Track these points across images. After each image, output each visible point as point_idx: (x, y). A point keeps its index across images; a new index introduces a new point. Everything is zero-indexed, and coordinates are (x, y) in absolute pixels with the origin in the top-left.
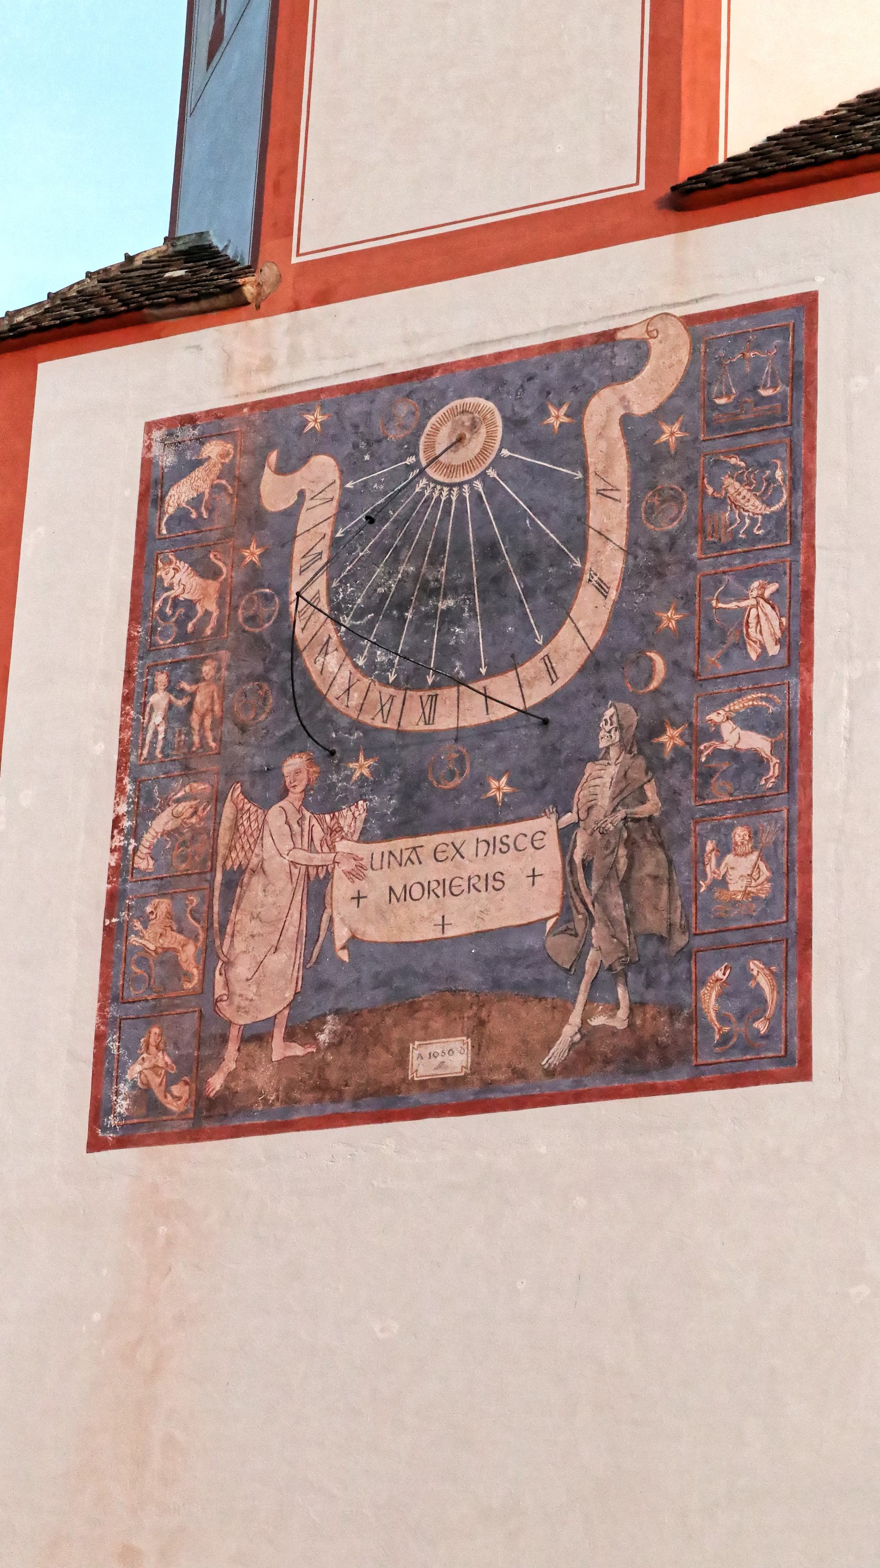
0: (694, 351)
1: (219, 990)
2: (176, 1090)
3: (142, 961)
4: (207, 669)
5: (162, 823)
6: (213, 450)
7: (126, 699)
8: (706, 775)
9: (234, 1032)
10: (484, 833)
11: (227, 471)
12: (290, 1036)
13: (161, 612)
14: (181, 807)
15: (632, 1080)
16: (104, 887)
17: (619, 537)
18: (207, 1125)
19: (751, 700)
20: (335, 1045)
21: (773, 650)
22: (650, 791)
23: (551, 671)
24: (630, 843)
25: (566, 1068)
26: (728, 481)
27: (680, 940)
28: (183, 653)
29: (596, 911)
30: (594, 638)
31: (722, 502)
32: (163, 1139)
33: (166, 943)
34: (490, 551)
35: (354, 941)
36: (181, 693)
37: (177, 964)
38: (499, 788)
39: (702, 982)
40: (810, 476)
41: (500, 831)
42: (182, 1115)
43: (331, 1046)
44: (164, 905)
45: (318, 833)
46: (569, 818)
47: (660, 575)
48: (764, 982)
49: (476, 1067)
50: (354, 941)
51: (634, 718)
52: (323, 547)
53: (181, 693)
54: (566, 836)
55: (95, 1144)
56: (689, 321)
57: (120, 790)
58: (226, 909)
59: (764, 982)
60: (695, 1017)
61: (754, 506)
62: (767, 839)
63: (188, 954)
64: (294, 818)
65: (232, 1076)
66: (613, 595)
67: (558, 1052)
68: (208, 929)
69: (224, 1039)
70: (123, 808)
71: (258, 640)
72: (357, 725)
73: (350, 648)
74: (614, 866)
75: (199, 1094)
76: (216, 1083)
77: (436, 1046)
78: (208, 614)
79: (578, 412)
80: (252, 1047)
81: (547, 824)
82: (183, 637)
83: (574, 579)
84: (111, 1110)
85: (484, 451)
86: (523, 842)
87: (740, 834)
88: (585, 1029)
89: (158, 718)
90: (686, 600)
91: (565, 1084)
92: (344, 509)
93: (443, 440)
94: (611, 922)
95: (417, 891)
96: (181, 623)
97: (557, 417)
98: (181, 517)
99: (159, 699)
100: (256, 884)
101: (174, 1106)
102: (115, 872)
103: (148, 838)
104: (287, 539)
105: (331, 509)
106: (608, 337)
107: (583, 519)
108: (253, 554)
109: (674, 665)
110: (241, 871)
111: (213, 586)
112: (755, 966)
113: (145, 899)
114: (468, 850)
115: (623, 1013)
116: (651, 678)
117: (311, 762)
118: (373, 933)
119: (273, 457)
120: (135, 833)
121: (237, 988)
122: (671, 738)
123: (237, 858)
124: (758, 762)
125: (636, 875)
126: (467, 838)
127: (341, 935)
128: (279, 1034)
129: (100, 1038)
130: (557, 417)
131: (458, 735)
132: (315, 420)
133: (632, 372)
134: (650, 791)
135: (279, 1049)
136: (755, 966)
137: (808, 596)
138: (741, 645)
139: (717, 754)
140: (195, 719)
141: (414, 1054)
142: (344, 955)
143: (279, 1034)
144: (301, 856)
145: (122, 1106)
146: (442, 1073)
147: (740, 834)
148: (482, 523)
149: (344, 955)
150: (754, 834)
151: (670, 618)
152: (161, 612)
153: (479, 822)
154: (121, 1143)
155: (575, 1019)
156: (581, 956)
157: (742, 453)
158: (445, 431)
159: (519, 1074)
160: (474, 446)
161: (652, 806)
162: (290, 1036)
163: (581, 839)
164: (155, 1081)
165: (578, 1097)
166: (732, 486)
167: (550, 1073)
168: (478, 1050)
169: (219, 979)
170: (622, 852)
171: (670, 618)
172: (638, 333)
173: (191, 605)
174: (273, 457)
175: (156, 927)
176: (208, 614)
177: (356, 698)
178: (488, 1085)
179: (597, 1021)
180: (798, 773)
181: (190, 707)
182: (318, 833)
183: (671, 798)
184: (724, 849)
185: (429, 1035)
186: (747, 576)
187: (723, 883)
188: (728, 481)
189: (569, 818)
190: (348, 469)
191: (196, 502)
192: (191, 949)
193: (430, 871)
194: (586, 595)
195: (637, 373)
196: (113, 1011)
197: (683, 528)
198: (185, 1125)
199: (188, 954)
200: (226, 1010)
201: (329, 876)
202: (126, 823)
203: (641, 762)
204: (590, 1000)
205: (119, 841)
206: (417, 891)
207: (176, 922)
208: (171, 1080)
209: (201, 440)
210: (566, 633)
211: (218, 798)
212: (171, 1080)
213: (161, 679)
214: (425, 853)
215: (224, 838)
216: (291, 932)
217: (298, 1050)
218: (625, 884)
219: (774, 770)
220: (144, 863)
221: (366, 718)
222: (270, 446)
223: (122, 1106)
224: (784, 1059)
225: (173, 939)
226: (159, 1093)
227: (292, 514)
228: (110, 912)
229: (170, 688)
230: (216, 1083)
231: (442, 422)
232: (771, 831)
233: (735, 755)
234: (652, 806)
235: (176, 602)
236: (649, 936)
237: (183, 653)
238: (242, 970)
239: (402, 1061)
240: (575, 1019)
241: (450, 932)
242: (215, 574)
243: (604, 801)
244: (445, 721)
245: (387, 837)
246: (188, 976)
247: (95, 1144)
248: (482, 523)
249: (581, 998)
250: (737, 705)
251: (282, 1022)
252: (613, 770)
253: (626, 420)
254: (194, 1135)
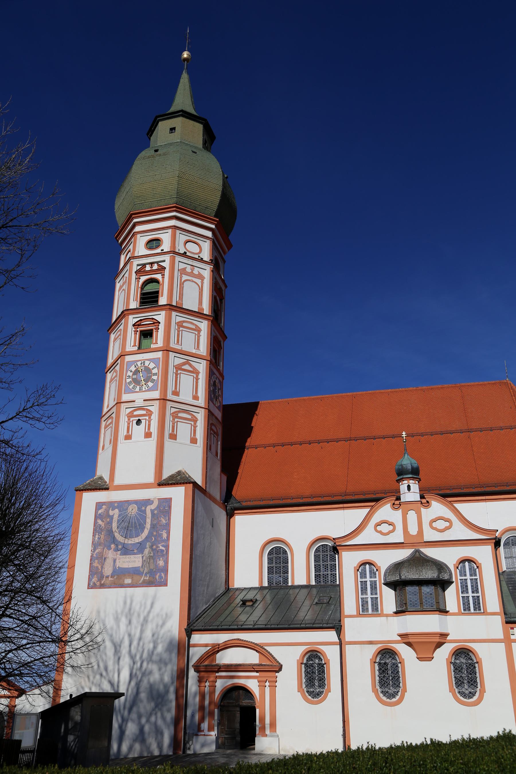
0: (159, 503)
1: (103, 571)
2: (98, 583)
3: (94, 567)
4: (103, 533)
5: (97, 551)
6: (104, 507)
7: (93, 536)
8: (158, 552)
9: (105, 577)
10: (134, 556)
11: (105, 509)
12: (111, 577)
13: (97, 526)
14: (99, 549)
15: (148, 585)
16: (90, 558)
17: (150, 523)
18: (101, 587)
19: (163, 544)
20: (116, 579)
21: (166, 538)
22: (152, 553)
23: (142, 538)
24: (149, 559)
25: (142, 583)
26: (162, 518)
27: (154, 570)
28: (100, 531)
29: (145, 566)
30: (147, 534)
31: (161, 521)
32: (96, 588)
33: (97, 565)
34: (135, 523)
35: (119, 567)
36: (99, 536)
37: (98, 568)
38: (136, 551)
39: (156, 575)
40: (170, 519)
41: (135, 556)
42: (98, 586)
43: (116, 579)
44: (97, 561)
45: (115, 554)
46: (143, 555)
47: (154, 528)
48: (163, 575)
49: (132, 582)
50: (119, 567)
51: (150, 544)
52: (117, 520)
53: (99, 536)
54: (143, 557)
55: (88, 588)
56: (158, 499)
57: (92, 547)
58: (104, 562)
59: (163, 575)
60: (156, 579)
61: (164, 522)
62: (164, 559)
63: (100, 567)
64: (112, 552)
65: (104, 581)
66: (149, 530)
67: (141, 582)
68: (102, 564)
69: (104, 577)
70: (92, 549)
71: (109, 530)
72: (120, 542)
73: (119, 532)
74: (148, 561)
75: (100, 583)
76: (102, 582)
77: (128, 580)
78: (103, 526)
79: (146, 508)
80: (107, 578)
81: (140, 555)
82: (100, 529)
83: (144, 527)
84: (90, 584)
85: (135, 511)
86: (138, 557)
87: (161, 559)
88: (144, 579)
89: (97, 539)
90: (157, 532)
91: (141, 585)
92: (119, 516)
93: (130, 510)
94: (147, 567)
95: (126, 562)
96: (100, 527)
97: (143, 508)
98: (100, 514)
99: (97, 536)
100: (108, 559)
101: (98, 585)
102: (91, 556)
103: (95, 553)
104: (112, 519)
105: (118, 515)
106: (149, 499)
107: (146, 521)
108: (108, 520)
109: (155, 539)
110: (106, 558)
111: (104, 523)
112: (162, 574)
113: (95, 560)
114: (132, 557)
115: (148, 578)
116: (152, 540)
117: (115, 546)
118: (121, 566)
119: (111, 508)
120: (94, 552)
121: (105, 571)
122: (154, 547)
123: (106, 556)
124: (163, 551)
125: (150, 562)
126: (132, 556)
127: (117, 566)
128: (110, 577)
129: (89, 576)
130: (143, 508)
131: (131, 544)
132: (116, 505)
133: (151, 504)
134: (152, 553)
135: (110, 579)
136: (162, 574)
137: (170, 532)
138: (162, 537)
139: (159, 549)
140: (101, 539)
141: (125, 581)
142: (118, 568)
143: (110, 577)
144: (113, 556)
145: (92, 584)
146: (128, 583)
147: (161, 559)
148: (135, 520)
149: (118, 568)
150: (163, 559)
151: (155, 533)
152: (97, 526)
153: (133, 555)
154: (91, 588)
155: (143, 578)
156: (144, 571)
157: (163, 515)
158: (131, 508)
159: (136, 583)
160: (133, 511)
161: (152, 555)
162: (111, 577)
163: (144, 557)
164: (96, 582)
165: (143, 587)
166: (162, 519)
167: (140, 584)
168: (132, 581)
169: (103, 570)
170: (149, 560)
171: (155, 533)
172: (153, 500)
173: (101, 525)
174: (111, 508)
175: (96, 563)
176: (103, 526)
177: (120, 538)
178: (133, 585)
179: (145, 578)
180: (168, 552)
181: (101, 537)
182: (115, 554)
183: (154, 554)
184: (160, 560)
185: (127, 578)
186: (163, 530)
187: (159, 564)
188: (162, 518)
189: (143, 555)
190: (120, 511)
191: (102, 513)
192: (100, 566)
193: (128, 560)
194: (146, 530)
195: (152, 504)
196: (90, 573)
197: (157, 523)
198: (99, 587)
199: (100, 567)
200: (104, 574)
201: (116, 559)
202: (93, 551)
203: (151, 550)
204: (144, 576)
205: (92, 553)
206: (126, 562)
207: (98, 563)
208: (97, 581)
209: (102, 505)
210: (143, 534)
211: (104, 549)
212: (97, 581)
213: (97, 534)
214: (127, 557)
215: (104, 554)
216: (112, 565)
217: (112, 579)
218: (149, 563)
219: (165, 552)
220: (95, 555)
221: (121, 541)
222: (110, 507)
223: (92, 584)
224: (165, 584)
225: (98, 565)
226: (96, 583)
227: (113, 516)
228: (90, 561)
229: (98, 535)
230: (102, 582)
231: (131, 507)
232: (165, 559)
233: (161, 549)
234: (152, 555)
235: (99, 525)
236: (151, 569)
237: (100, 531)
238: (106, 569)
239: (124, 581)
240: (143, 578)
241: (129, 567)
242: (104, 522)
243: (147, 553)
244: (130, 542)
245: (123, 555)
246: (100, 569)
247: (88, 588)
248: (135, 520)
249: (144, 575)
250: (161, 544)
251: (110, 576)
252: (148, 550)
253: (151, 510)
254: (100, 588)
